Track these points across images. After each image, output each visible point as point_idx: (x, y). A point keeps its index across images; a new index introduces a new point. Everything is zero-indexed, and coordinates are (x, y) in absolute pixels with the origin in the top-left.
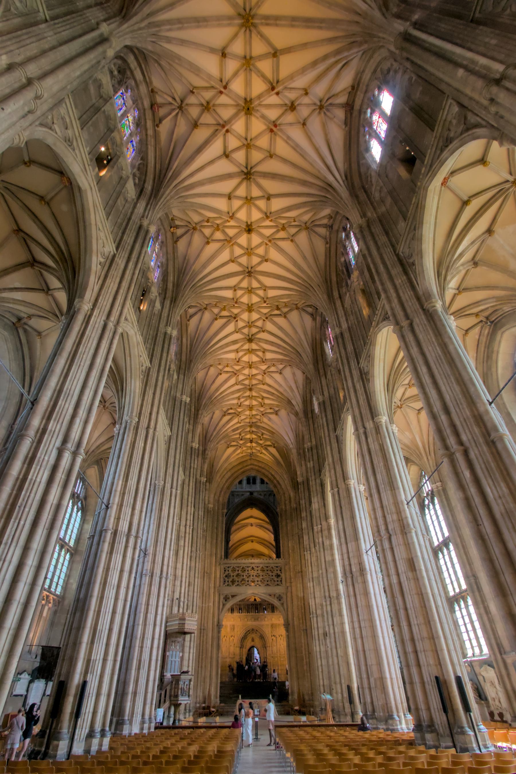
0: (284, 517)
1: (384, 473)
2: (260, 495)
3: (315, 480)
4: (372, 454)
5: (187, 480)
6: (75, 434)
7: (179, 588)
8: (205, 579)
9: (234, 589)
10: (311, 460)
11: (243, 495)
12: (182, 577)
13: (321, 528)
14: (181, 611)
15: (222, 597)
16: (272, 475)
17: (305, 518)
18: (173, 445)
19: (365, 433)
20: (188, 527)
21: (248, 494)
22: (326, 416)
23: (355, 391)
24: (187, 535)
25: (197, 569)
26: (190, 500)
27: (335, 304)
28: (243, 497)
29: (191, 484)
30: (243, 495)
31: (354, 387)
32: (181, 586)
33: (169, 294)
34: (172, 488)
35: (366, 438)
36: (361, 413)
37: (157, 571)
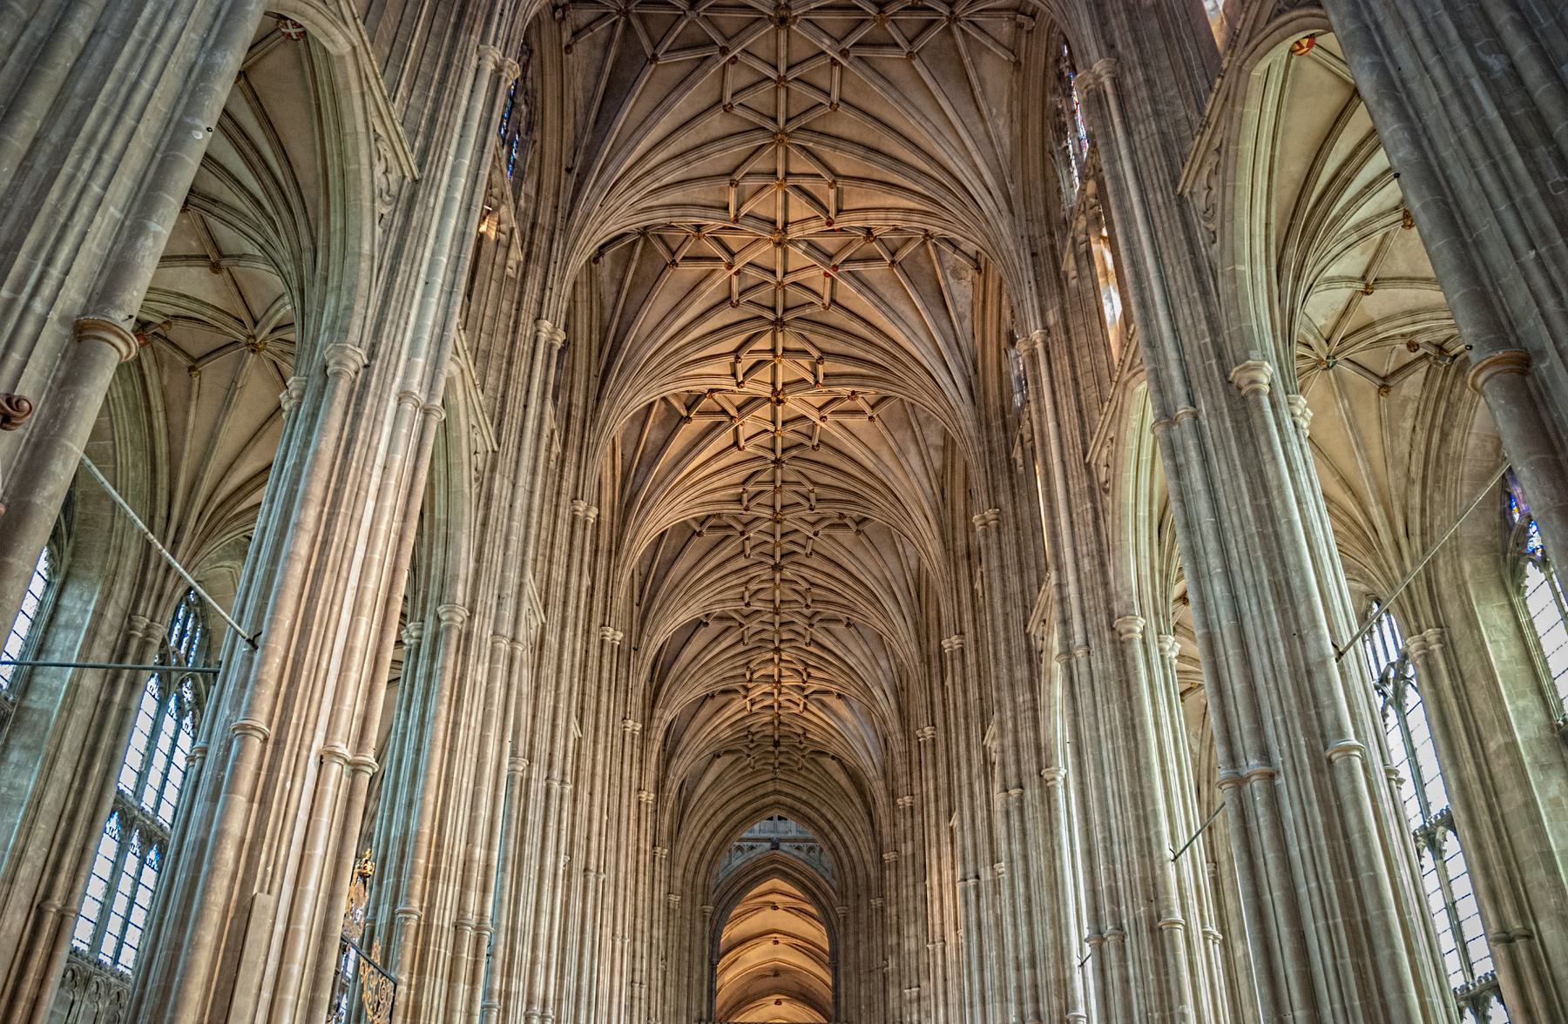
0: (851, 929)
1: (996, 972)
2: (798, 848)
3: (914, 886)
4: (984, 930)
6: (539, 991)
10: (909, 836)
11: (752, 848)
13: (919, 993)
16: (828, 822)
17: (895, 949)
19: (977, 887)
21: (767, 845)
22: (936, 778)
23: (972, 796)
24: (636, 1002)
27: (956, 565)
28: (752, 854)
29: (640, 890)
30: (752, 848)
31: (971, 784)
33: (604, 543)
35: (978, 897)
36: (975, 845)
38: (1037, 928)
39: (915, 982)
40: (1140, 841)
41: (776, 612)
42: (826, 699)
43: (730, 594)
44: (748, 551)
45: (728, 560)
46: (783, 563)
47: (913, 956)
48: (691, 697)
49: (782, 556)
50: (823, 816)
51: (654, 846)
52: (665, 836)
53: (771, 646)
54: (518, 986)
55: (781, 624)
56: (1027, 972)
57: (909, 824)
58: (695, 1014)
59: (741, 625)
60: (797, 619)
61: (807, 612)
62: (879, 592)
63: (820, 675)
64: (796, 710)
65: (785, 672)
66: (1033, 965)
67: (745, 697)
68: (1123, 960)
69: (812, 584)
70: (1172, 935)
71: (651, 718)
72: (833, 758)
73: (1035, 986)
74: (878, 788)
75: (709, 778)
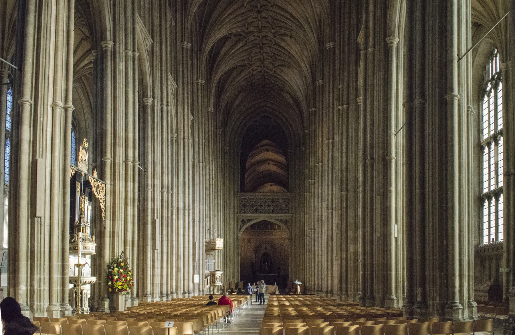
5: (207, 142)
7: (209, 223)
8: (226, 208)
9: (249, 216)
12: (210, 215)
13: (314, 181)
14: (212, 237)
15: (240, 221)
18: (196, 128)
19: (333, 143)
20: (211, 180)
25: (219, 205)
26: (211, 159)
32: (210, 221)
34: (199, 162)
35: (333, 147)
37: (197, 218)
38: (349, 158)
39: (313, 177)
40: (384, 126)
41: (260, 31)
42: (283, 68)
43: (239, 24)
44: (245, 5)
45: (236, 10)
46: (262, 9)
47: (313, 168)
48: (226, 69)
49: (261, 7)
50: (283, 116)
51: (216, 129)
52: (220, 124)
53: (259, 46)
54: (158, 182)
55: (263, 37)
56: (344, 174)
57: (313, 119)
58: (236, 190)
59: (245, 38)
60: (269, 34)
61: (273, 31)
62: (301, 20)
63: (280, 58)
64: (271, 73)
65: (266, 57)
66: (347, 171)
67: (249, 68)
68: (372, 170)
69: (274, 19)
70: (390, 162)
71: (210, 78)
72: (287, 92)
73: (347, 179)
74: (303, 105)
75: (237, 102)
